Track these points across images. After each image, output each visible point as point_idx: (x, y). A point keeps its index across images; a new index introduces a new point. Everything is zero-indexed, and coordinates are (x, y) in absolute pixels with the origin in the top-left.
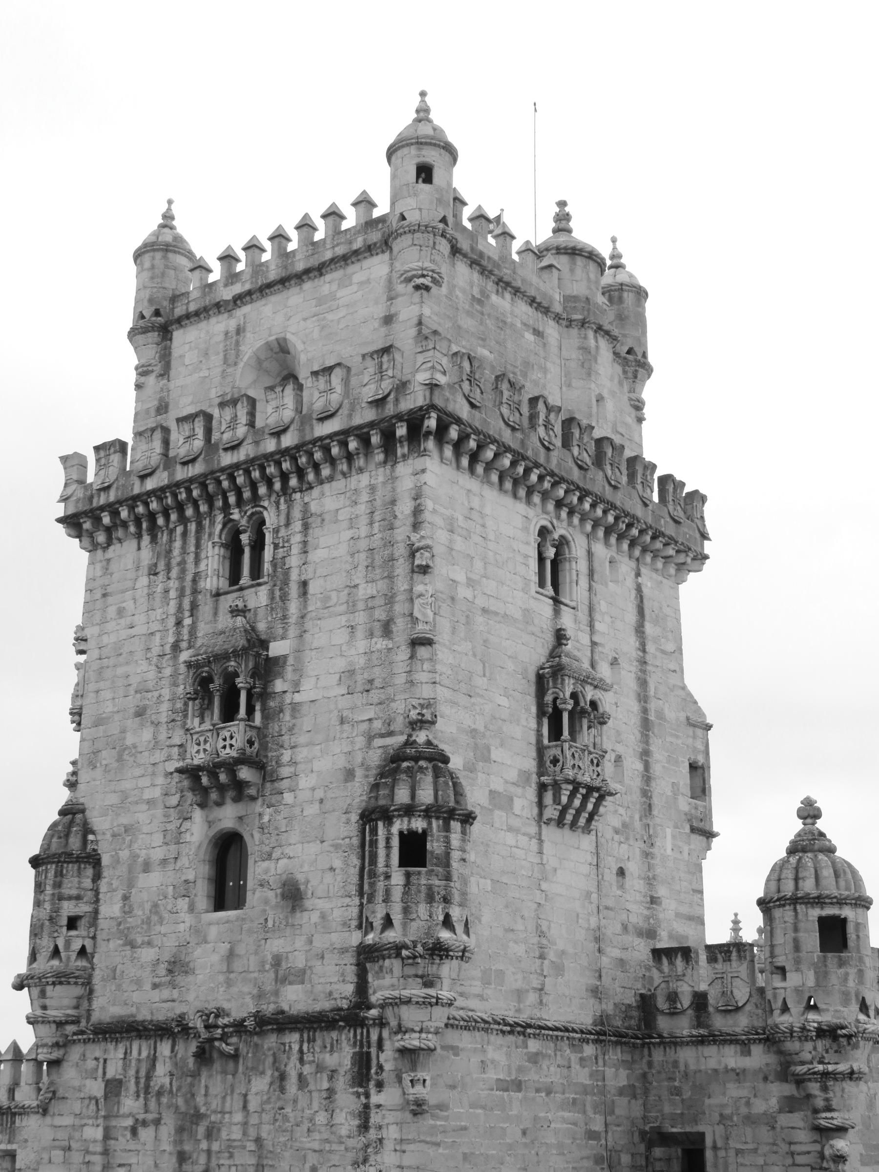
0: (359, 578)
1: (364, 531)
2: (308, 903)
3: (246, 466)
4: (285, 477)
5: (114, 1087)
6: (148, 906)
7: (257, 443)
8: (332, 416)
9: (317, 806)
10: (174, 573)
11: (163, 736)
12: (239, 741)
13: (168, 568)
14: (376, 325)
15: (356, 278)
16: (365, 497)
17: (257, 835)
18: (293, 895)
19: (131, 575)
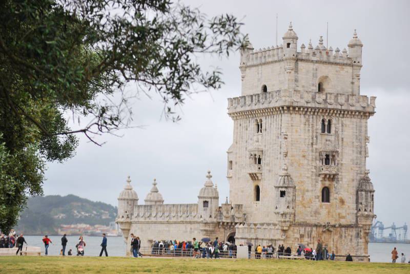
0: (354, 141)
1: (355, 131)
2: (345, 203)
3: (334, 110)
4: (339, 114)
5: (302, 236)
6: (308, 199)
7: (336, 105)
9: (346, 185)
10: (311, 126)
12: (336, 170)
13: (309, 125)
14: (350, 83)
15: (345, 70)
16: (355, 124)
17: (334, 189)
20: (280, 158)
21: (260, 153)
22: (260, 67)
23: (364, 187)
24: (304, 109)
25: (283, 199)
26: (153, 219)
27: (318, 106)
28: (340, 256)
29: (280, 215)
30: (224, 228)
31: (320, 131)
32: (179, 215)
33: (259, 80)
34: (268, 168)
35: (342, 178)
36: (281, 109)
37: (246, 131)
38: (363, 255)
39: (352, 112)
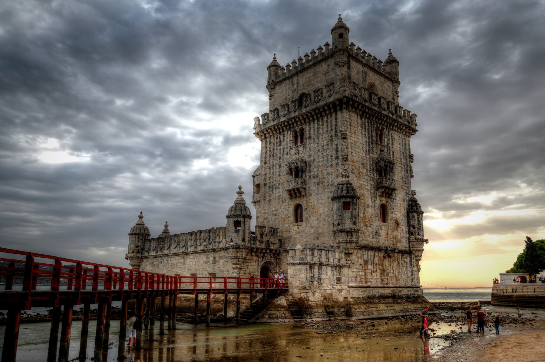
2: (400, 226)
5: (366, 262)
8: (401, 118)
11: (369, 173)
18: (397, 223)
19: (356, 123)
20: (337, 164)
21: (303, 165)
22: (295, 78)
23: (414, 210)
24: (362, 107)
25: (347, 214)
26: (166, 252)
27: (373, 107)
28: (400, 287)
29: (344, 234)
30: (258, 256)
31: (374, 139)
32: (198, 243)
33: (293, 91)
34: (316, 180)
35: (395, 196)
36: (337, 103)
37: (279, 148)
38: (417, 285)
39: (400, 125)
